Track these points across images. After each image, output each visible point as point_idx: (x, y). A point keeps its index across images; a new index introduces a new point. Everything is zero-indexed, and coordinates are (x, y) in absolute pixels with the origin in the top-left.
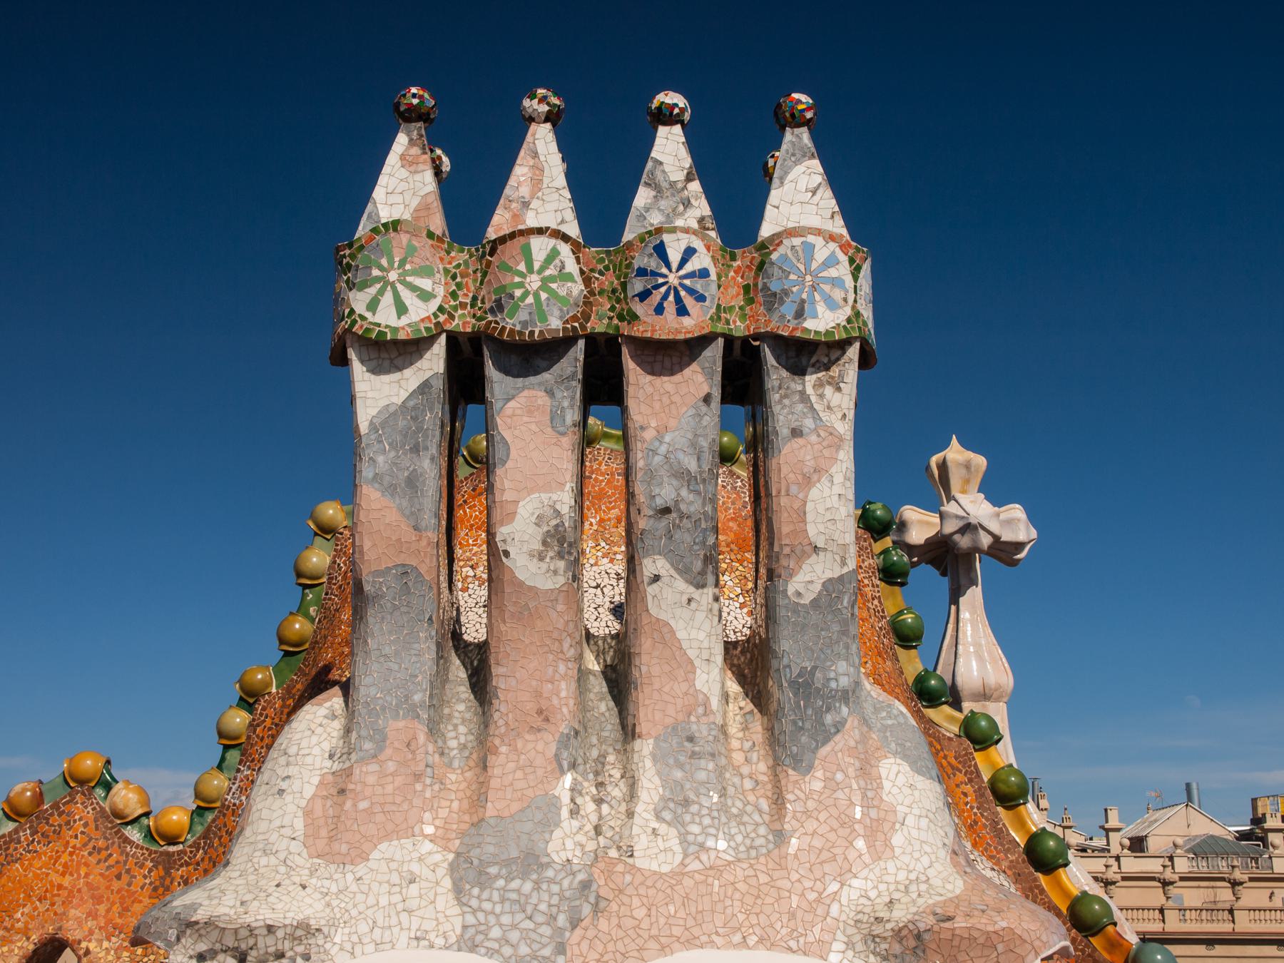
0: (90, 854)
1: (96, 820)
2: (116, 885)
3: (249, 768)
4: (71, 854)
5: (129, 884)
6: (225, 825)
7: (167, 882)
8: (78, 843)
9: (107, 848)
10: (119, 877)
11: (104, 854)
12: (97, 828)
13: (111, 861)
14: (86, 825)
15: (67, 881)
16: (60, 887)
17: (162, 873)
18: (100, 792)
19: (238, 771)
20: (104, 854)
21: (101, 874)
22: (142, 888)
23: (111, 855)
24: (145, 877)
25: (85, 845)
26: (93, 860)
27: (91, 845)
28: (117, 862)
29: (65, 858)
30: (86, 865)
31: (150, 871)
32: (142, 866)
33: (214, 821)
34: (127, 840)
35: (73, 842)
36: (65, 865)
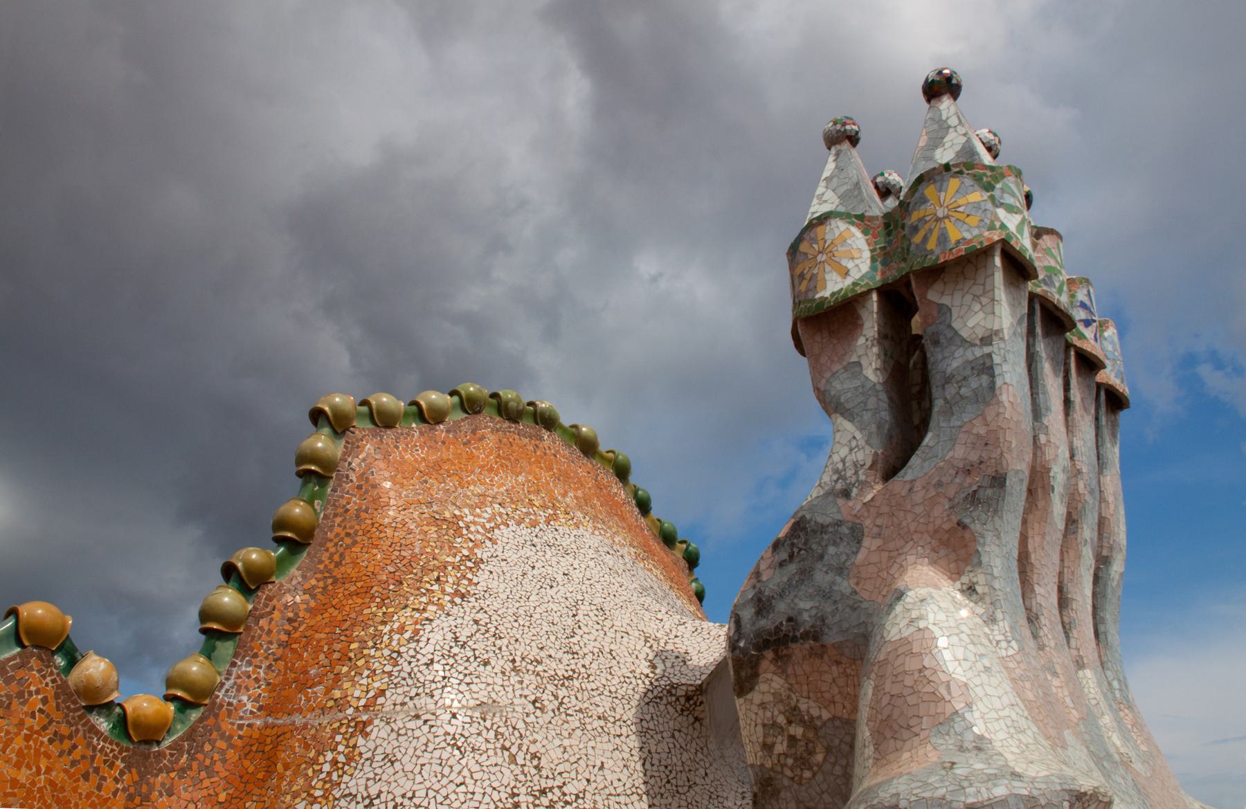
0: (51, 741)
1: (57, 696)
2: (84, 787)
3: (249, 663)
4: (27, 738)
5: (99, 788)
6: (219, 729)
7: (144, 789)
8: (35, 723)
9: (70, 737)
10: (86, 777)
11: (67, 744)
12: (58, 708)
13: (77, 754)
14: (45, 701)
15: (23, 775)
16: (14, 783)
17: (136, 778)
18: (60, 661)
19: (234, 664)
20: (67, 744)
21: (66, 771)
22: (115, 794)
23: (75, 747)
24: (117, 780)
25: (44, 728)
26: (54, 749)
27: (52, 729)
28: (83, 757)
29: (18, 743)
30: (48, 756)
31: (122, 773)
32: (112, 766)
33: (201, 720)
34: (93, 730)
35: (29, 721)
36: (20, 753)
